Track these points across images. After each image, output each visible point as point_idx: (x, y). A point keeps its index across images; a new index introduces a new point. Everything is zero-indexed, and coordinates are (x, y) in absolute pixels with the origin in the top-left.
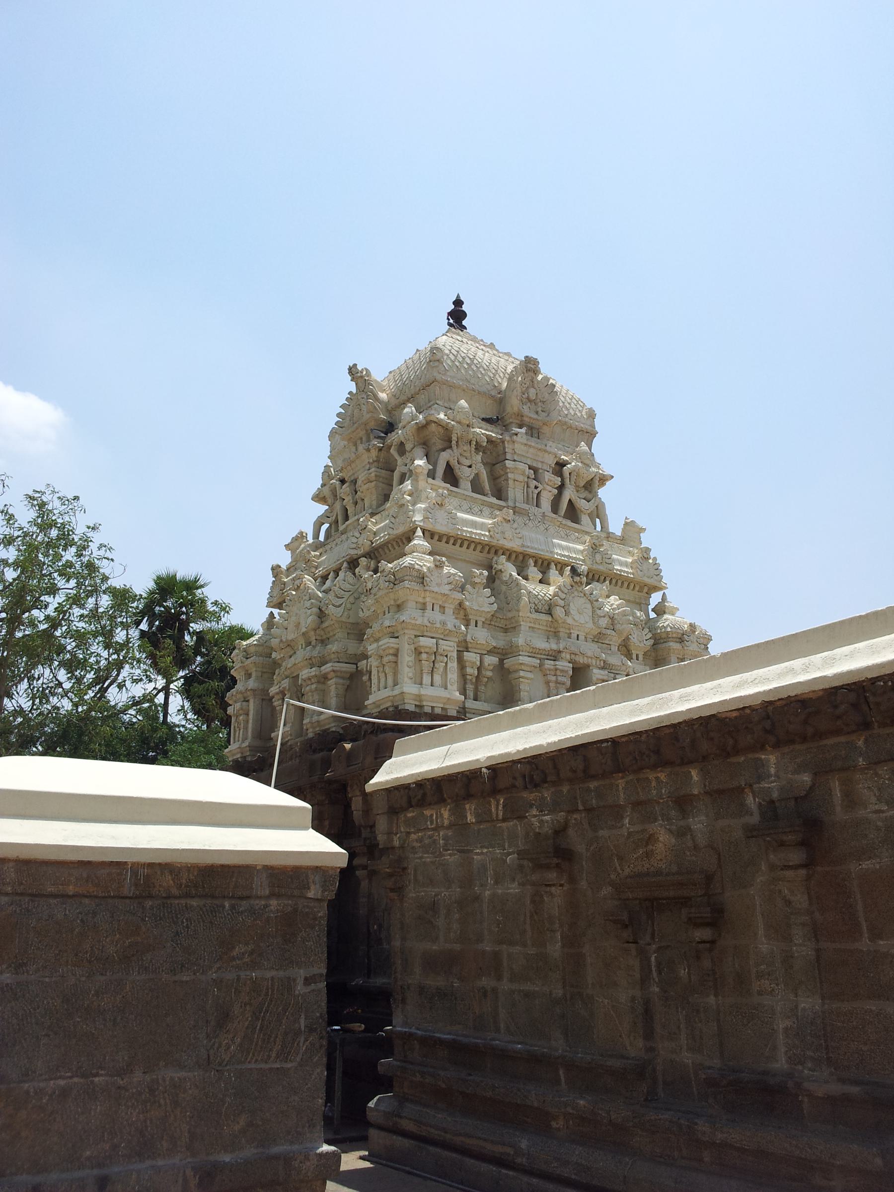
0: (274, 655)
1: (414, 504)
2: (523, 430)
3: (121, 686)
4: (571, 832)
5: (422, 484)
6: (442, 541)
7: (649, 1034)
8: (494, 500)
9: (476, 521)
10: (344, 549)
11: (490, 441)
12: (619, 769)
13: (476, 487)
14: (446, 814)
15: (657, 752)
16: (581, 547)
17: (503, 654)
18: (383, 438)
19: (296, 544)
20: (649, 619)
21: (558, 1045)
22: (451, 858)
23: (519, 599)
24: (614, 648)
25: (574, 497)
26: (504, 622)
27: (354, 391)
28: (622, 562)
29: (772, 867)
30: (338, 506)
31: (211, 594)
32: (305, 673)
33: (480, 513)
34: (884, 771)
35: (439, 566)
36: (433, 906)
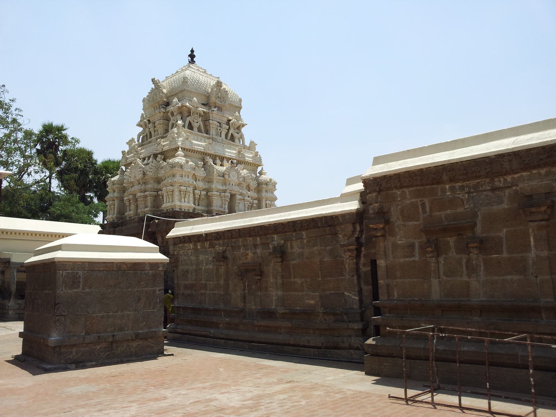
0: (124, 185)
1: (178, 138)
2: (216, 109)
3: (29, 175)
4: (227, 252)
5: (181, 130)
6: (189, 152)
7: (245, 302)
8: (205, 135)
9: (199, 144)
10: (151, 149)
11: (204, 112)
12: (240, 236)
13: (199, 130)
14: (192, 246)
15: (250, 233)
16: (235, 152)
17: (208, 190)
18: (165, 109)
19: (131, 143)
20: (257, 176)
21: (222, 306)
22: (193, 258)
23: (213, 172)
24: (245, 188)
25: (233, 132)
26: (208, 180)
27: (154, 88)
28: (249, 156)
29: (274, 262)
30: (147, 130)
31: (70, 133)
32: (139, 194)
33: (201, 141)
34: (299, 241)
35: (187, 162)
36: (187, 271)
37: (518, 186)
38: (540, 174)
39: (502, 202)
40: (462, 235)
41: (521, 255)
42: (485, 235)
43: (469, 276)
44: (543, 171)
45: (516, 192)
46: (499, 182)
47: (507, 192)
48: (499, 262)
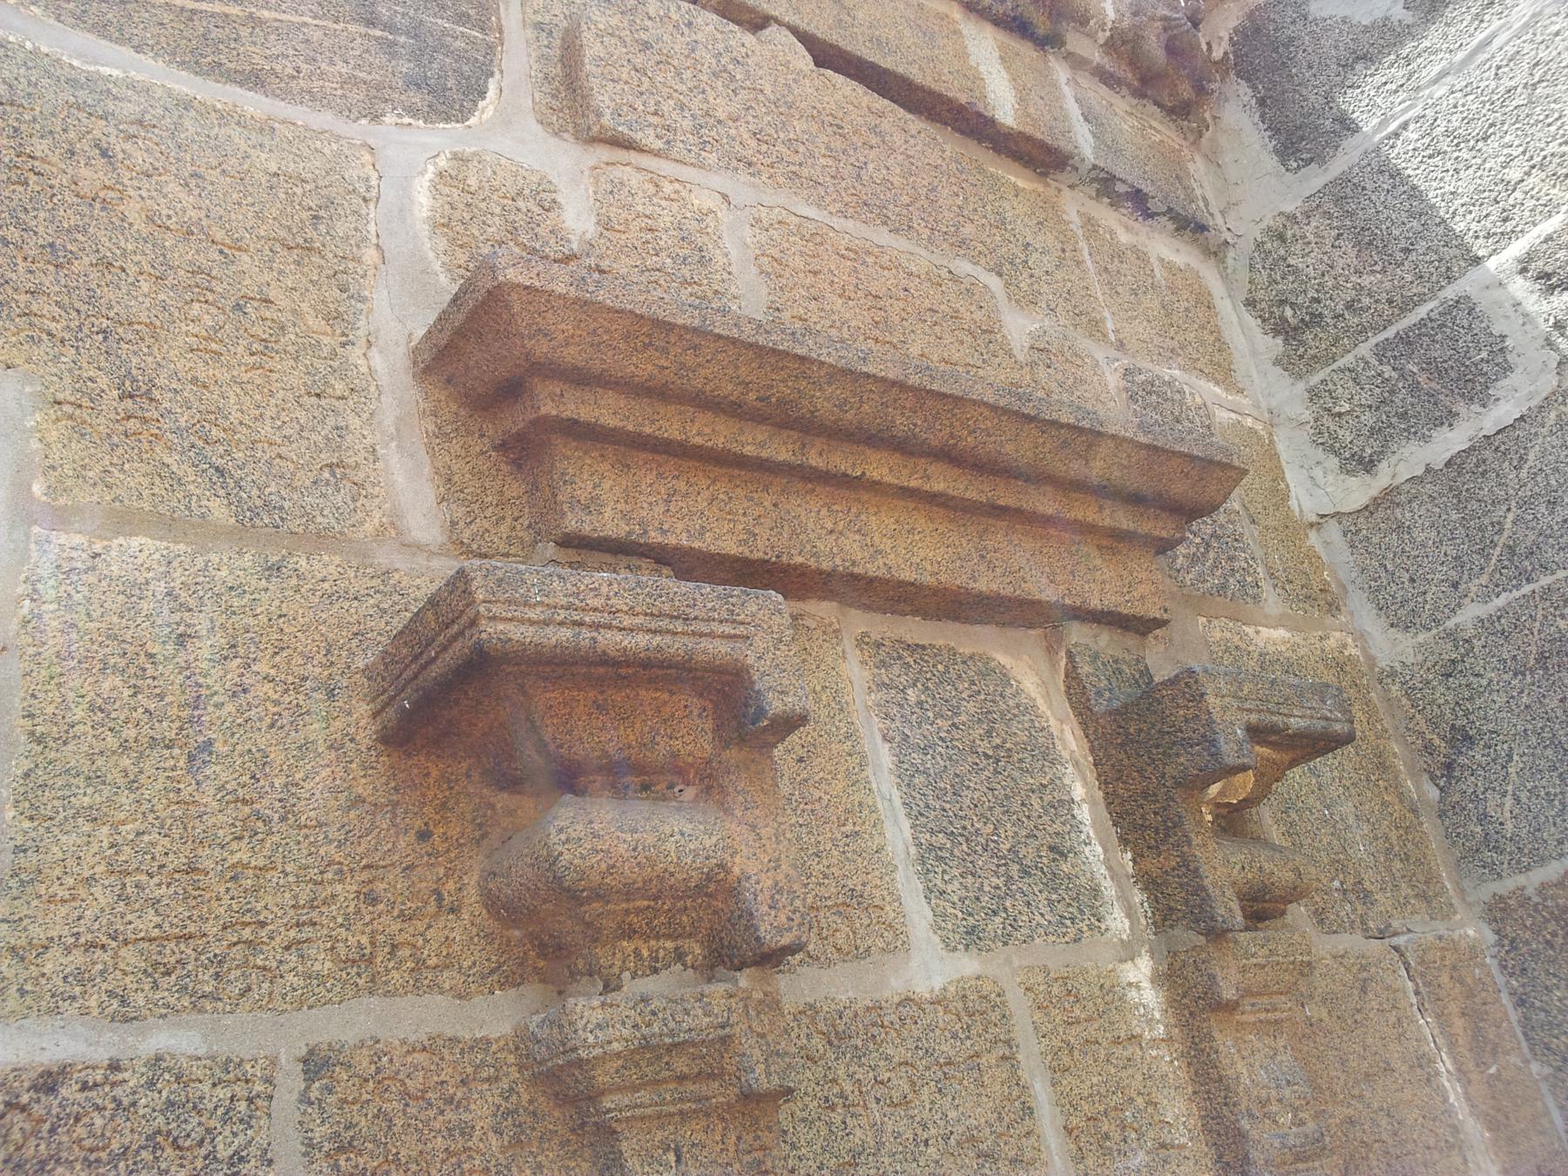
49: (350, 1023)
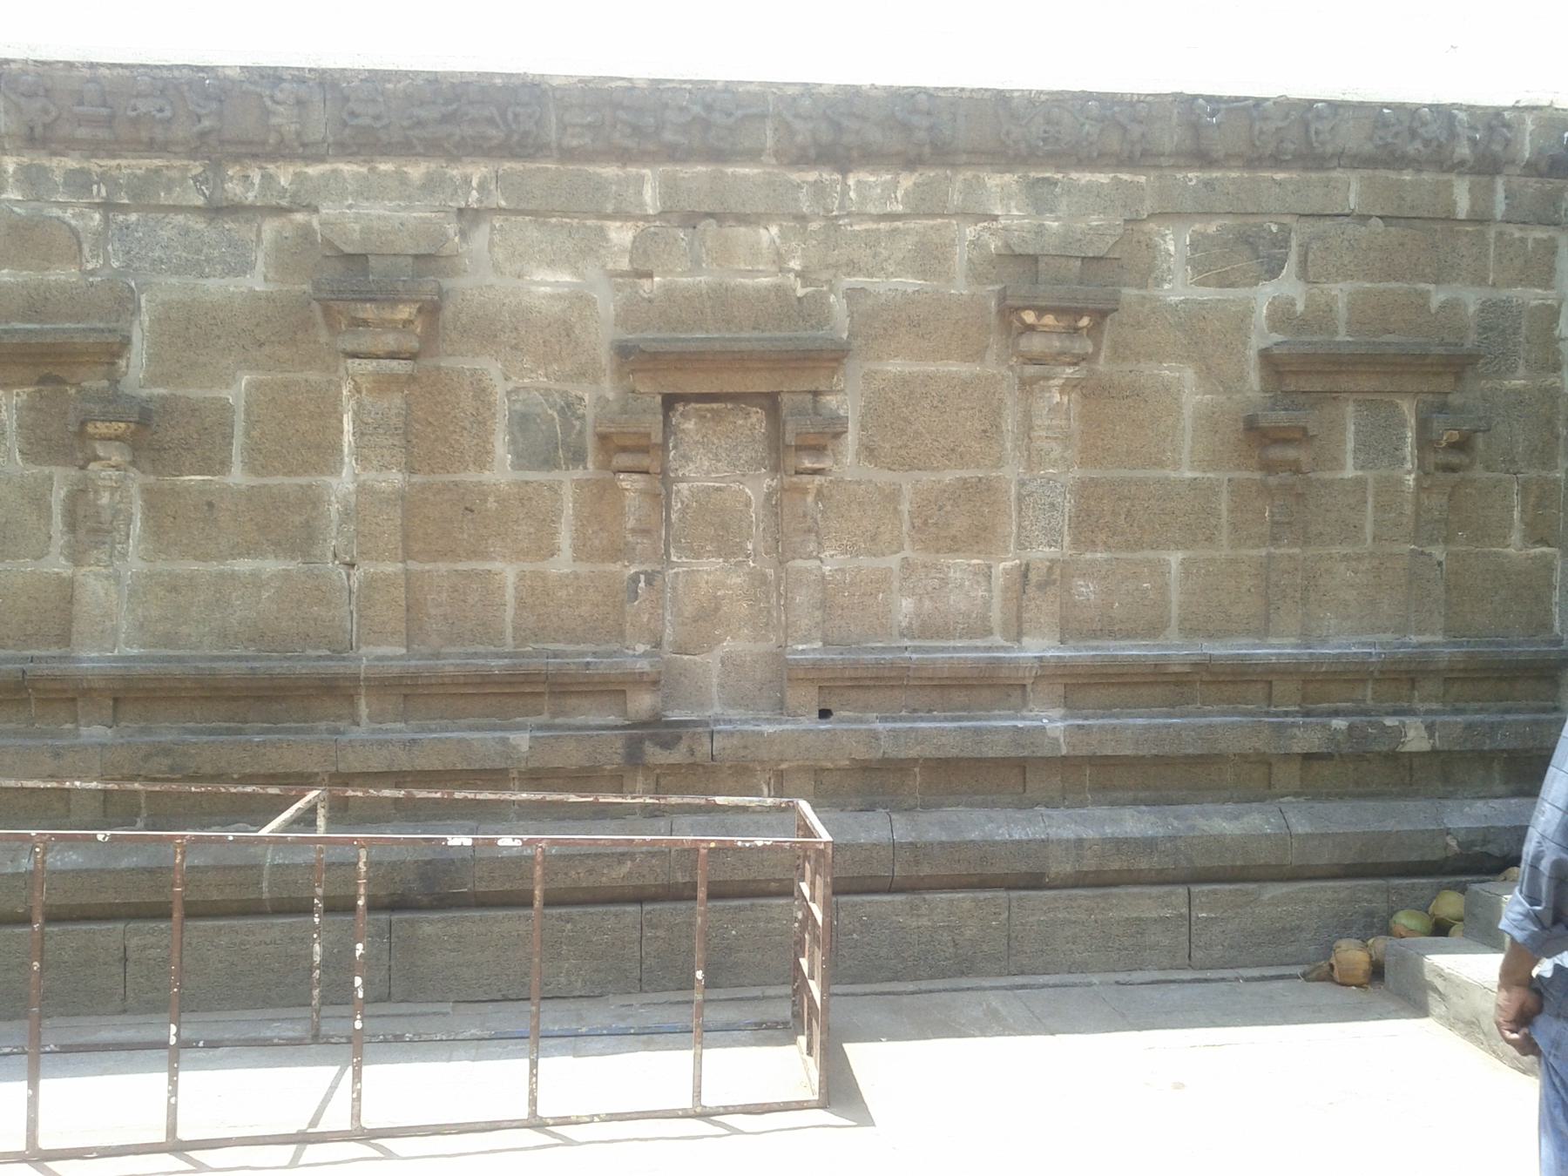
37: (316, 210)
38: (403, 180)
39: (245, 267)
40: (59, 381)
41: (303, 480)
42: (162, 391)
43: (76, 556)
44: (417, 171)
45: (306, 233)
46: (244, 183)
47: (270, 227)
48: (210, 505)
49: (1237, 475)
